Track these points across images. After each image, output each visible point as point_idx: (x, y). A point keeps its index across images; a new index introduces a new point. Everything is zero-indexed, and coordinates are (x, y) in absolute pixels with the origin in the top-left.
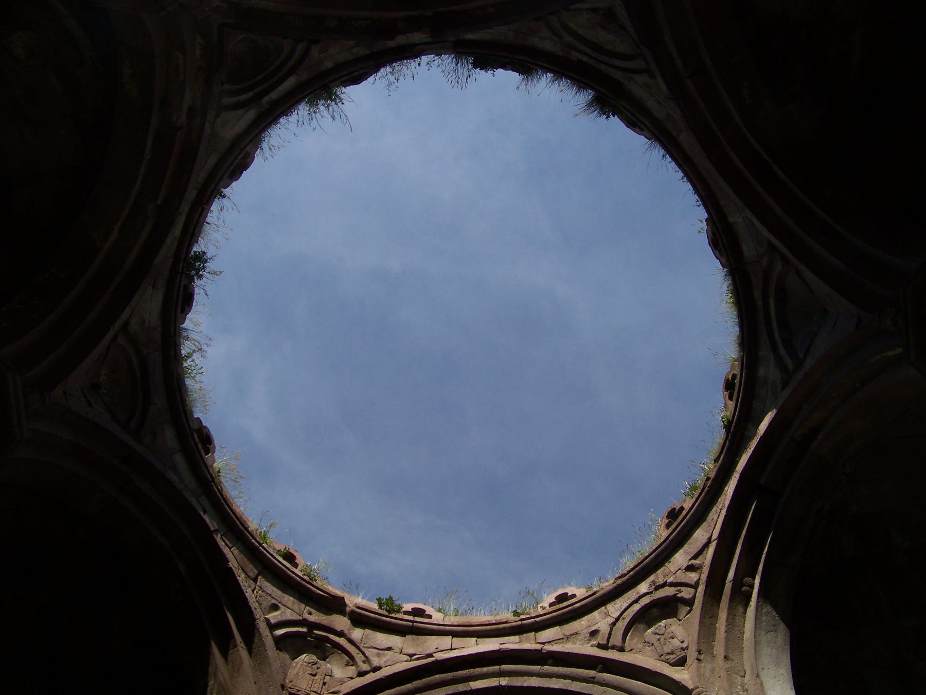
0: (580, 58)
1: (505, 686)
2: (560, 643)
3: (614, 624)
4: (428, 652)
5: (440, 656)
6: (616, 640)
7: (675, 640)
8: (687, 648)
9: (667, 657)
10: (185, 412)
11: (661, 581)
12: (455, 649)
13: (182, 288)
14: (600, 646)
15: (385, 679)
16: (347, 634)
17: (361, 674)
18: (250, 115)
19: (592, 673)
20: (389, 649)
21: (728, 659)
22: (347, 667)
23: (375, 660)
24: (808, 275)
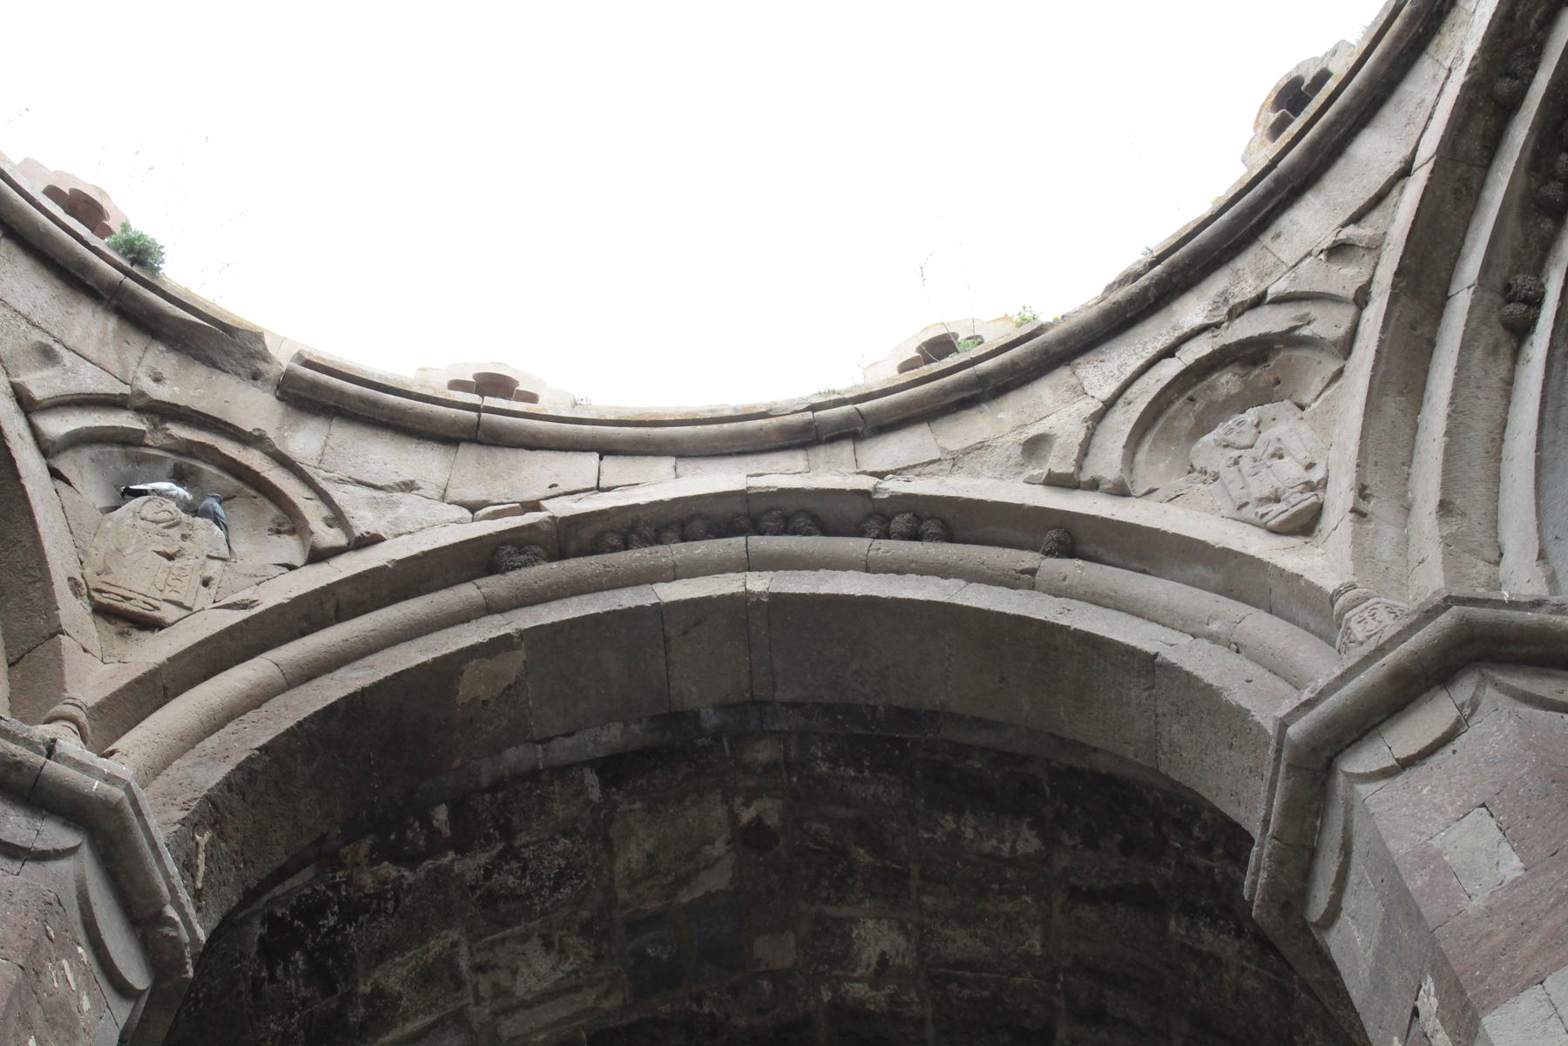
1: (761, 594)
2: (932, 474)
3: (1099, 417)
6: (1108, 461)
7: (1287, 459)
8: (1324, 483)
9: (1261, 510)
11: (1248, 291)
12: (609, 489)
14: (1056, 482)
17: (318, 556)
19: (1029, 559)
20: (409, 487)
21: (1450, 511)
22: (275, 538)
23: (363, 518)
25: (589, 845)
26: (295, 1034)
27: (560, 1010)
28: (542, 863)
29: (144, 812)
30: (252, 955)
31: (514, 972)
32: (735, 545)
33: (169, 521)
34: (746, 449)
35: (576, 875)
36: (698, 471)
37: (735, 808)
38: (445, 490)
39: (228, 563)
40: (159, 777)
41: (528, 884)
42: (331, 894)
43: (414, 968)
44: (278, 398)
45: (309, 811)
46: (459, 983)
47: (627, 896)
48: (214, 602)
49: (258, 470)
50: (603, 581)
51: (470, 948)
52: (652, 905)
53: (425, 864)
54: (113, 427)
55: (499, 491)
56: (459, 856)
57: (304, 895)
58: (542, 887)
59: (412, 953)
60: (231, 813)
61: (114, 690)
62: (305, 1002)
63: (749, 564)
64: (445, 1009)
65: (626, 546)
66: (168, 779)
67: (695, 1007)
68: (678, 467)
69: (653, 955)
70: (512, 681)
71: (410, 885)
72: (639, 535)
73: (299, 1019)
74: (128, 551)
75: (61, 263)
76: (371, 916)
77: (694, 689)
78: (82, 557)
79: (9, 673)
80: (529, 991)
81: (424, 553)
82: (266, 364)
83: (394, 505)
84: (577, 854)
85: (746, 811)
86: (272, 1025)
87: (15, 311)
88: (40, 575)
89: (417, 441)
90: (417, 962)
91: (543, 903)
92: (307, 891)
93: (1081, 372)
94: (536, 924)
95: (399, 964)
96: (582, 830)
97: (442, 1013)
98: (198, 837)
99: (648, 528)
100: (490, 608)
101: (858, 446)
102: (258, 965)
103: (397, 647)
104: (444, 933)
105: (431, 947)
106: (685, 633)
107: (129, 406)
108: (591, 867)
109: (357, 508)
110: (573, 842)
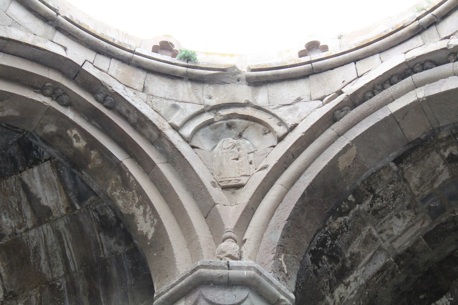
1: (423, 98)
4: (337, 89)
5: (349, 90)
12: (362, 76)
15: (305, 135)
16: (253, 102)
17: (280, 139)
20: (299, 100)
22: (265, 136)
23: (289, 119)
25: (399, 183)
26: (332, 279)
27: (411, 232)
28: (387, 195)
29: (262, 272)
30: (310, 265)
31: (392, 229)
32: (408, 81)
33: (232, 146)
34: (401, 41)
35: (399, 193)
36: (388, 56)
37: (442, 154)
38: (311, 96)
39: (255, 153)
40: (261, 242)
41: (385, 202)
42: (326, 235)
43: (360, 242)
44: (248, 85)
45: (309, 227)
46: (375, 239)
47: (418, 193)
48: (256, 169)
49: (252, 115)
50: (371, 111)
51: (375, 228)
52: (427, 192)
53: (351, 212)
54: (204, 122)
55: (327, 90)
56: (360, 205)
57: (318, 240)
58: (390, 202)
59: (358, 239)
60: (287, 244)
61: (238, 219)
62: (331, 269)
63: (416, 86)
64: (375, 249)
65: (374, 95)
66: (264, 242)
67: (453, 215)
68: (381, 57)
69: (433, 206)
70: (355, 157)
71: (349, 221)
72: (377, 90)
73: (332, 274)
74: (224, 163)
75: (167, 73)
76: (341, 235)
77: (413, 133)
78: (212, 172)
79: (206, 221)
80: (399, 232)
81: (312, 126)
82: (239, 74)
83: (296, 109)
84: (397, 188)
85: (445, 153)
86: (325, 280)
87: (161, 98)
88: (202, 187)
89: (296, 81)
90: (360, 240)
91: (392, 206)
92: (319, 238)
94: (393, 212)
95: (355, 243)
96: (396, 180)
97: (374, 250)
98: (280, 259)
99: (379, 86)
100: (339, 135)
101: (437, 26)
102: (313, 266)
103: (316, 161)
104: (365, 228)
105: (363, 234)
106: (403, 118)
107: (205, 111)
108: (403, 189)
109: (286, 116)
110: (394, 185)
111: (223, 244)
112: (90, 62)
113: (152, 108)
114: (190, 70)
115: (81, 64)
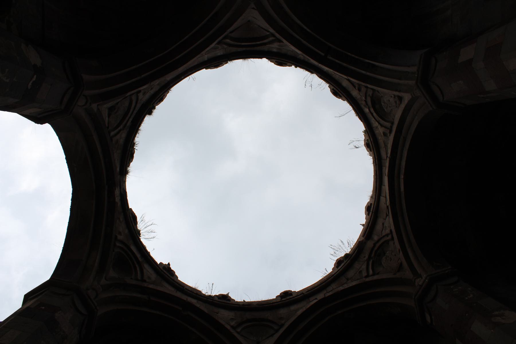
0: (130, 122)
6: (388, 125)
9: (398, 104)
10: (273, 303)
11: (364, 103)
12: (386, 196)
13: (220, 300)
14: (390, 132)
17: (393, 238)
18: (146, 266)
20: (383, 224)
24: (231, 29)
93: (374, 127)
111: (416, 284)
112: (326, 293)
113: (356, 280)
114: (351, 259)
115: (324, 297)
